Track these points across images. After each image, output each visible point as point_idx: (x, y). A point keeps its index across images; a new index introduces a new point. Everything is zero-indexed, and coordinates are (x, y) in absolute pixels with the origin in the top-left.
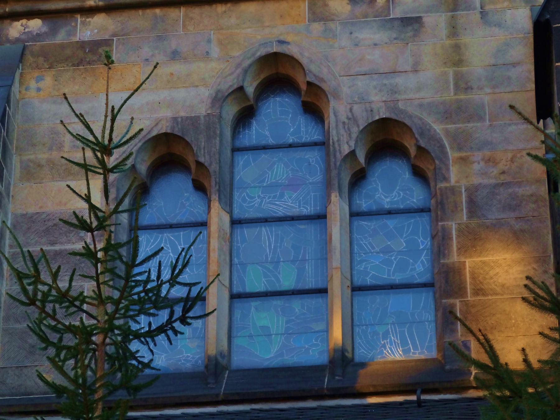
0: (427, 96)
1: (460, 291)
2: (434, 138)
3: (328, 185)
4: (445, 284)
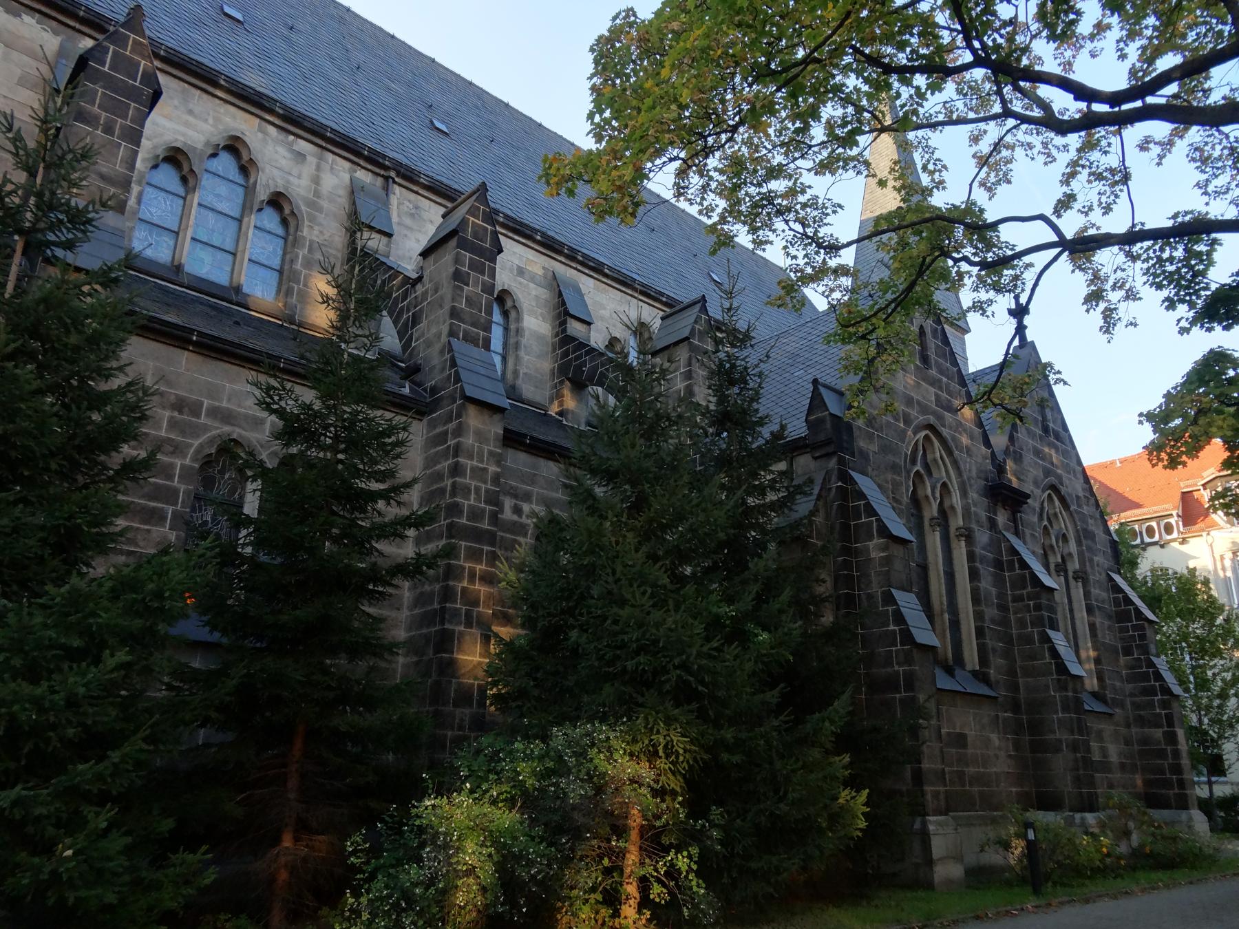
0: (302, 192)
1: (298, 282)
2: (300, 211)
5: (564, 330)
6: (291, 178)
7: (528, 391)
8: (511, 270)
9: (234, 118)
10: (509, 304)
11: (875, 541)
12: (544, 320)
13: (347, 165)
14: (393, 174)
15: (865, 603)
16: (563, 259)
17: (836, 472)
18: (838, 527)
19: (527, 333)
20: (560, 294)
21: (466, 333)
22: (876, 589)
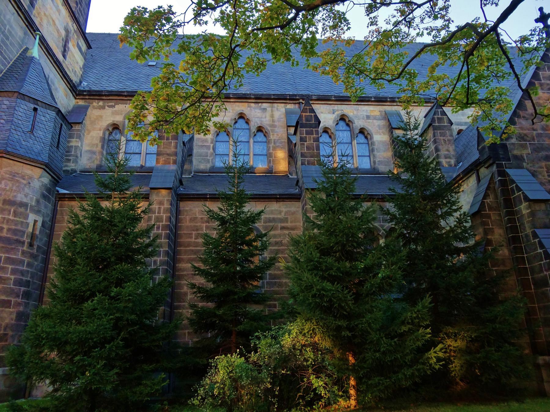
0: (268, 123)
1: (272, 157)
2: (268, 130)
3: (250, 136)
4: (269, 155)
5: (392, 137)
6: (263, 119)
7: (382, 168)
8: (363, 119)
9: (239, 106)
10: (366, 133)
11: (524, 204)
12: (384, 134)
13: (283, 105)
14: (301, 101)
15: (525, 239)
16: (389, 104)
17: (496, 172)
18: (502, 201)
19: (376, 143)
20: (389, 121)
21: (308, 161)
22: (529, 231)
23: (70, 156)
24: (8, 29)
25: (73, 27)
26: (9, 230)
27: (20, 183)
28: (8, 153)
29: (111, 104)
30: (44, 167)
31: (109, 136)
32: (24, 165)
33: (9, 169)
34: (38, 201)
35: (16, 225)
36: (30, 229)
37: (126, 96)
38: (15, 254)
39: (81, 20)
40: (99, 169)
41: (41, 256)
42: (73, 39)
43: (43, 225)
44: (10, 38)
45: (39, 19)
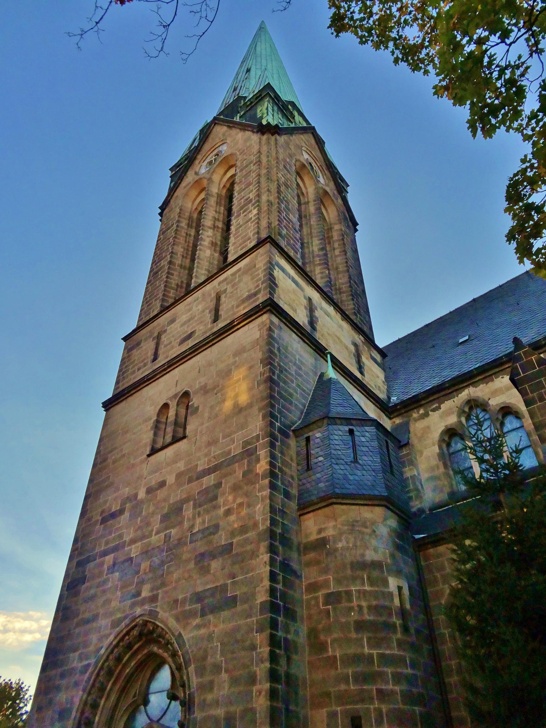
23: (408, 492)
24: (299, 359)
25: (359, 339)
26: (369, 607)
27: (363, 533)
28: (338, 496)
29: (434, 406)
30: (386, 503)
31: (448, 450)
32: (362, 508)
33: (344, 518)
34: (392, 556)
35: (376, 598)
36: (397, 602)
37: (448, 388)
38: (389, 647)
39: (365, 329)
40: (453, 496)
41: (426, 647)
42: (365, 351)
43: (411, 594)
44: (303, 368)
45: (324, 340)
